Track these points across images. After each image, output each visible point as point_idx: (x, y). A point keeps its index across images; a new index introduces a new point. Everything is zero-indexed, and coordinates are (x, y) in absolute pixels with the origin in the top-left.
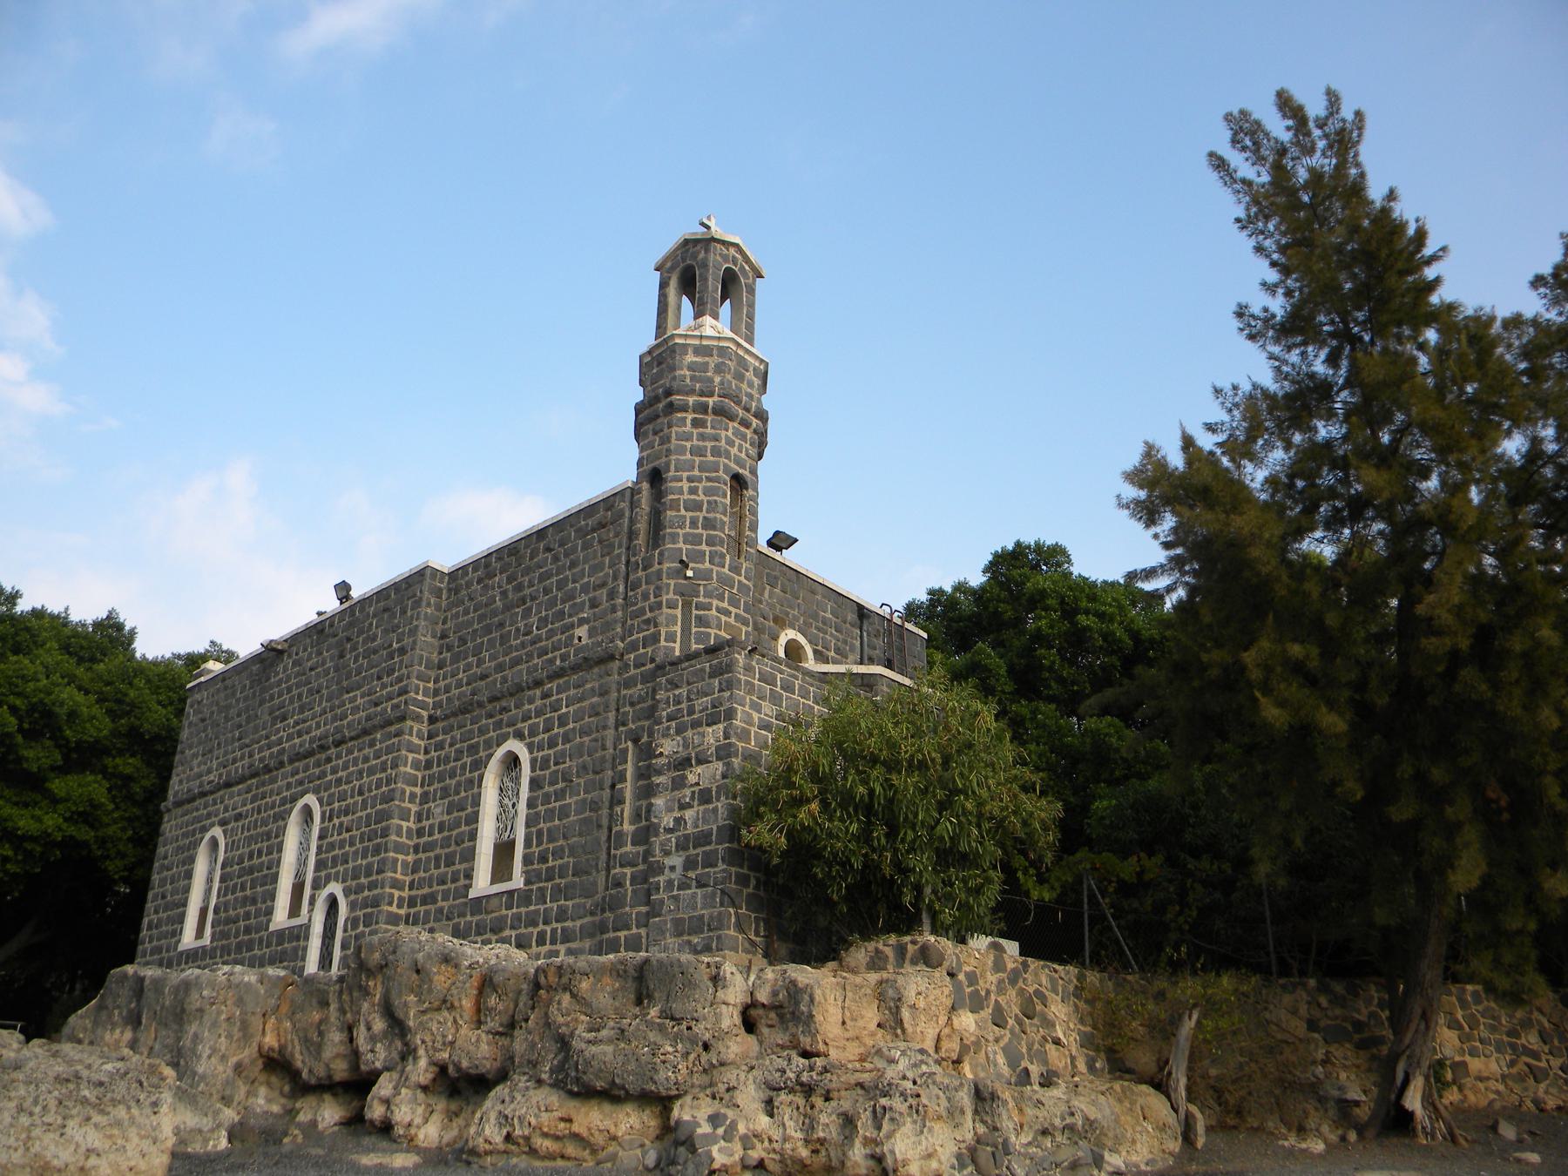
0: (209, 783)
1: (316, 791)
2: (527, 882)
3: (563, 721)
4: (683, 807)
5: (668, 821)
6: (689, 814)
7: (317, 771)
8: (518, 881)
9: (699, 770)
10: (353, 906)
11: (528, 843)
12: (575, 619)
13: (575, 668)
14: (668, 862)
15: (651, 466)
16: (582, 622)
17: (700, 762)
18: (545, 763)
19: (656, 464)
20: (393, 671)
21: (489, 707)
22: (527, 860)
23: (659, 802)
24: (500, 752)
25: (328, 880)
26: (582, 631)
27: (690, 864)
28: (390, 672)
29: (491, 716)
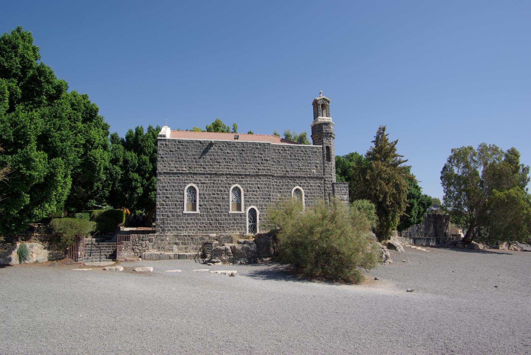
0: (184, 171)
1: (240, 184)
3: (311, 186)
9: (344, 202)
10: (261, 212)
12: (312, 168)
13: (315, 178)
15: (327, 145)
16: (314, 169)
17: (344, 200)
18: (308, 193)
19: (328, 145)
20: (264, 164)
21: (291, 179)
24: (295, 188)
25: (250, 205)
26: (314, 171)
29: (291, 180)
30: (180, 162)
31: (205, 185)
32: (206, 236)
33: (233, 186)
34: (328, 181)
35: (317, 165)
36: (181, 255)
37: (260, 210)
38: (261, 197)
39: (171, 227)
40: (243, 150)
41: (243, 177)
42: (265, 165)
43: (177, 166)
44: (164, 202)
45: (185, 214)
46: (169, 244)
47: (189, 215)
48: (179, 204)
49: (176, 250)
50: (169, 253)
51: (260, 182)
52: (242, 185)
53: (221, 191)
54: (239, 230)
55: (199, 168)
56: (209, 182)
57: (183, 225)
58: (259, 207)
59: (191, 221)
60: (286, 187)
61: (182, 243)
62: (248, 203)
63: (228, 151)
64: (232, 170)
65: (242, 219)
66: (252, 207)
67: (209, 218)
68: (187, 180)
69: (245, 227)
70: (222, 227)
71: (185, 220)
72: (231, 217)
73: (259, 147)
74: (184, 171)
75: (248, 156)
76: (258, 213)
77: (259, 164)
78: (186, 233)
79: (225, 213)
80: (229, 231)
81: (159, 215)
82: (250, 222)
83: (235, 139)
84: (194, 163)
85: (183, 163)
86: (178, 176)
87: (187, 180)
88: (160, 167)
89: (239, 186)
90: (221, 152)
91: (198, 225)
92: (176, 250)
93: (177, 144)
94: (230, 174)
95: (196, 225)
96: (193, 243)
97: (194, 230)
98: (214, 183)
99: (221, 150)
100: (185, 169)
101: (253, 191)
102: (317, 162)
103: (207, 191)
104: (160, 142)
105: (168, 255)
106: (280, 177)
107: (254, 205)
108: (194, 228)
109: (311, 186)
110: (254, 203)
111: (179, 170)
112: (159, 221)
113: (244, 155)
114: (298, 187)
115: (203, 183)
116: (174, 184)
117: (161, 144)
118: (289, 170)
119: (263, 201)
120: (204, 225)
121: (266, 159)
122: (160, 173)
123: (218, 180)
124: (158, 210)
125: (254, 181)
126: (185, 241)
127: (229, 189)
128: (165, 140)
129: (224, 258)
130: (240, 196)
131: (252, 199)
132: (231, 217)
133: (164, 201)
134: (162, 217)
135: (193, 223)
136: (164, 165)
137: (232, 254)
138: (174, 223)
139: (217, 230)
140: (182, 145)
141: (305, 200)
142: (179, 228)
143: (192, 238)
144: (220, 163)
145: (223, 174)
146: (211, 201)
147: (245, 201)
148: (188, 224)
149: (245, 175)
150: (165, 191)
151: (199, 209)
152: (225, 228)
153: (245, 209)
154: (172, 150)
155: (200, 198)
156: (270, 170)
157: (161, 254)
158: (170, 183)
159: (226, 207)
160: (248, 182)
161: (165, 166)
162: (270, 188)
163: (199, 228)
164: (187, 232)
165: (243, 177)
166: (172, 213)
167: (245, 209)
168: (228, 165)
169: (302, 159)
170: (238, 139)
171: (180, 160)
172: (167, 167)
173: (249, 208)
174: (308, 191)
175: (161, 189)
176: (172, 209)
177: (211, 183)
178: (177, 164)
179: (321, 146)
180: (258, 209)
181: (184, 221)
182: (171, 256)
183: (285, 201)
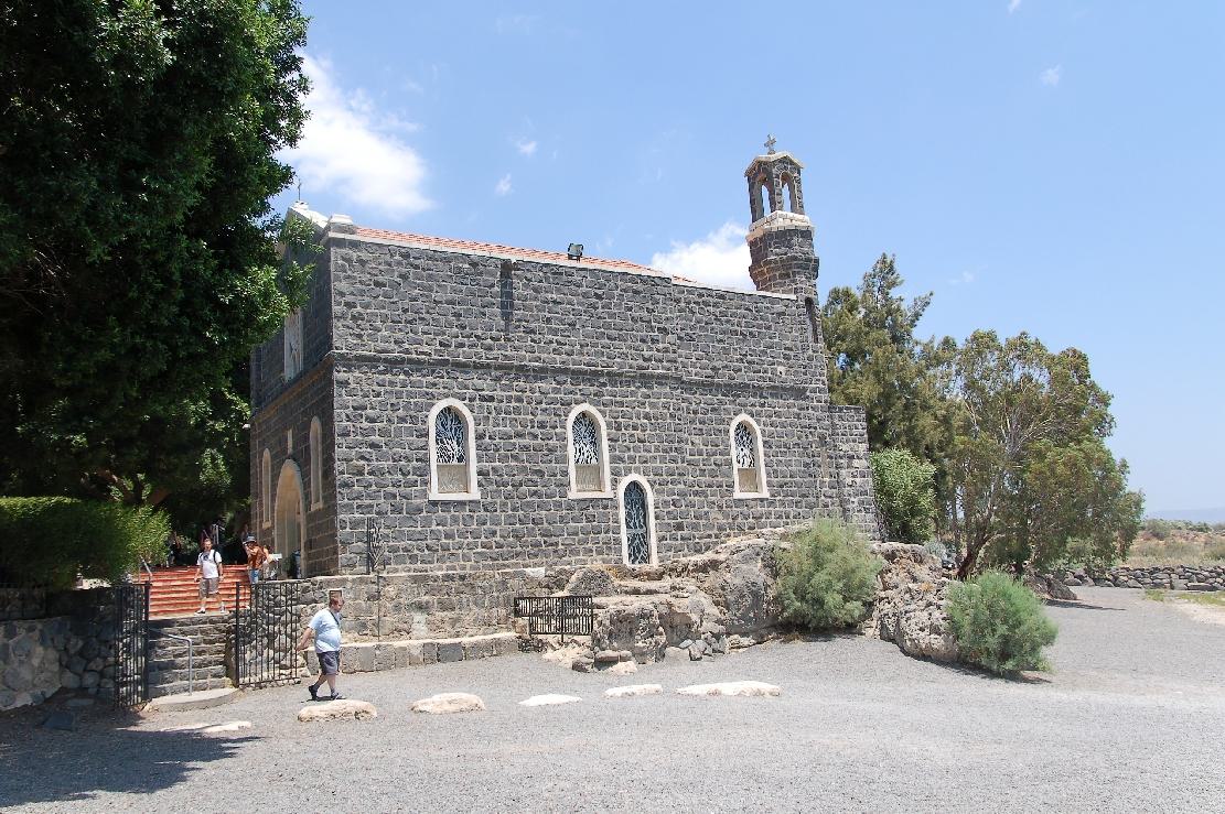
0: (422, 353)
2: (773, 495)
3: (777, 414)
4: (854, 477)
5: (849, 480)
6: (858, 480)
7: (593, 389)
8: (765, 493)
11: (768, 474)
14: (852, 499)
16: (780, 364)
22: (769, 484)
23: (843, 472)
25: (628, 471)
27: (861, 503)
28: (654, 341)
30: (410, 322)
31: (493, 405)
32: (515, 575)
33: (576, 410)
34: (818, 401)
35: (787, 352)
36: (445, 646)
37: (657, 487)
38: (657, 450)
39: (393, 550)
40: (598, 297)
41: (602, 380)
42: (661, 346)
43: (399, 335)
44: (362, 462)
45: (435, 503)
46: (397, 608)
47: (446, 503)
48: (414, 468)
49: (421, 634)
50: (403, 643)
51: (652, 400)
52: (602, 408)
53: (542, 425)
54: (600, 553)
55: (470, 346)
56: (503, 393)
57: (429, 541)
58: (652, 476)
59: (455, 528)
60: (714, 416)
61: (444, 607)
62: (622, 465)
63: (554, 296)
64: (570, 358)
65: (605, 515)
66: (633, 477)
67: (510, 516)
68: (435, 385)
69: (618, 542)
70: (552, 545)
71: (438, 525)
72: (576, 513)
73: (640, 287)
74: (422, 353)
75: (612, 316)
76: (651, 498)
77: (643, 341)
78: (441, 569)
79: (557, 498)
80: (573, 558)
81: (349, 508)
82: (628, 526)
83: (570, 257)
84: (455, 330)
85: (421, 328)
86: (406, 373)
87: (435, 385)
88: (342, 340)
89: (593, 410)
90: (536, 299)
91: (480, 541)
92: (421, 634)
93: (399, 263)
94: (565, 371)
95: (470, 540)
96: (476, 604)
97: (466, 558)
98: (519, 400)
99: (535, 290)
100: (426, 349)
101: (635, 428)
102: (788, 343)
103: (498, 425)
104: (338, 250)
105: (404, 649)
106: (698, 384)
107: (637, 470)
108: (466, 551)
109: (777, 414)
110: (637, 464)
111: (407, 352)
112: (348, 529)
113: (600, 310)
114: (743, 417)
115: (483, 399)
116: (394, 401)
117: (344, 259)
118: (718, 364)
119: (663, 460)
120: (498, 539)
121: (660, 326)
122: (350, 363)
123: (533, 392)
124: (345, 491)
125: (633, 394)
126: (447, 595)
127: (563, 417)
128: (355, 245)
129: (640, 644)
130: (595, 443)
131: (632, 453)
132: (576, 513)
133: (363, 458)
134: (357, 515)
135: (462, 535)
136: (357, 331)
137: (661, 629)
138: (399, 537)
139: (536, 556)
140: (417, 267)
141: (765, 455)
142: (416, 552)
143: (473, 587)
144: (533, 332)
145: (542, 370)
146: (515, 458)
147: (614, 459)
148: (448, 536)
149: (609, 374)
150: (366, 424)
151: (480, 484)
152: (560, 547)
153: (615, 482)
154: (380, 279)
155: (478, 447)
156: (675, 362)
157: (378, 647)
158: (379, 395)
159: (559, 477)
160: (618, 399)
161: (360, 336)
162: (680, 420)
163: (479, 550)
164: (444, 566)
165: (602, 380)
166: (392, 501)
167: (615, 482)
168: (559, 343)
169: (751, 333)
170: (578, 259)
171: (410, 316)
172: (365, 338)
173: (625, 482)
174: (769, 428)
175: (352, 417)
176: (393, 486)
177: (509, 399)
178: (400, 330)
179: (793, 297)
180: (652, 485)
181: (434, 527)
182: (416, 652)
183: (712, 458)
